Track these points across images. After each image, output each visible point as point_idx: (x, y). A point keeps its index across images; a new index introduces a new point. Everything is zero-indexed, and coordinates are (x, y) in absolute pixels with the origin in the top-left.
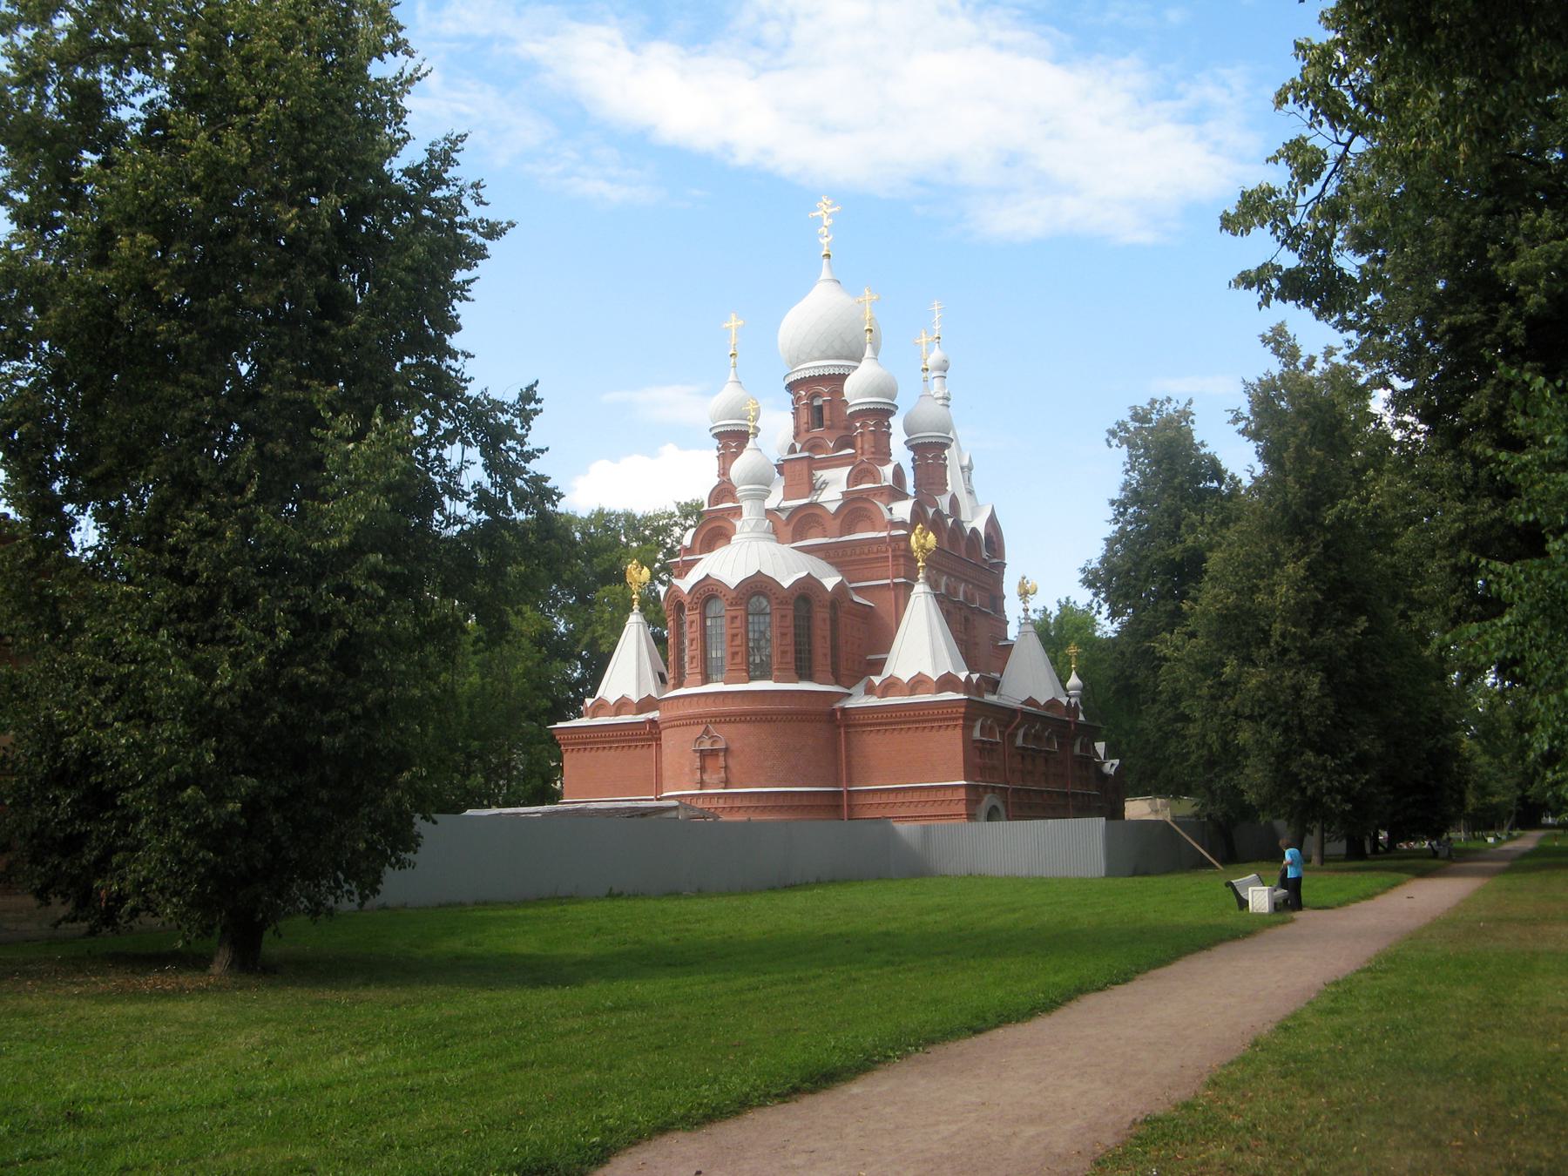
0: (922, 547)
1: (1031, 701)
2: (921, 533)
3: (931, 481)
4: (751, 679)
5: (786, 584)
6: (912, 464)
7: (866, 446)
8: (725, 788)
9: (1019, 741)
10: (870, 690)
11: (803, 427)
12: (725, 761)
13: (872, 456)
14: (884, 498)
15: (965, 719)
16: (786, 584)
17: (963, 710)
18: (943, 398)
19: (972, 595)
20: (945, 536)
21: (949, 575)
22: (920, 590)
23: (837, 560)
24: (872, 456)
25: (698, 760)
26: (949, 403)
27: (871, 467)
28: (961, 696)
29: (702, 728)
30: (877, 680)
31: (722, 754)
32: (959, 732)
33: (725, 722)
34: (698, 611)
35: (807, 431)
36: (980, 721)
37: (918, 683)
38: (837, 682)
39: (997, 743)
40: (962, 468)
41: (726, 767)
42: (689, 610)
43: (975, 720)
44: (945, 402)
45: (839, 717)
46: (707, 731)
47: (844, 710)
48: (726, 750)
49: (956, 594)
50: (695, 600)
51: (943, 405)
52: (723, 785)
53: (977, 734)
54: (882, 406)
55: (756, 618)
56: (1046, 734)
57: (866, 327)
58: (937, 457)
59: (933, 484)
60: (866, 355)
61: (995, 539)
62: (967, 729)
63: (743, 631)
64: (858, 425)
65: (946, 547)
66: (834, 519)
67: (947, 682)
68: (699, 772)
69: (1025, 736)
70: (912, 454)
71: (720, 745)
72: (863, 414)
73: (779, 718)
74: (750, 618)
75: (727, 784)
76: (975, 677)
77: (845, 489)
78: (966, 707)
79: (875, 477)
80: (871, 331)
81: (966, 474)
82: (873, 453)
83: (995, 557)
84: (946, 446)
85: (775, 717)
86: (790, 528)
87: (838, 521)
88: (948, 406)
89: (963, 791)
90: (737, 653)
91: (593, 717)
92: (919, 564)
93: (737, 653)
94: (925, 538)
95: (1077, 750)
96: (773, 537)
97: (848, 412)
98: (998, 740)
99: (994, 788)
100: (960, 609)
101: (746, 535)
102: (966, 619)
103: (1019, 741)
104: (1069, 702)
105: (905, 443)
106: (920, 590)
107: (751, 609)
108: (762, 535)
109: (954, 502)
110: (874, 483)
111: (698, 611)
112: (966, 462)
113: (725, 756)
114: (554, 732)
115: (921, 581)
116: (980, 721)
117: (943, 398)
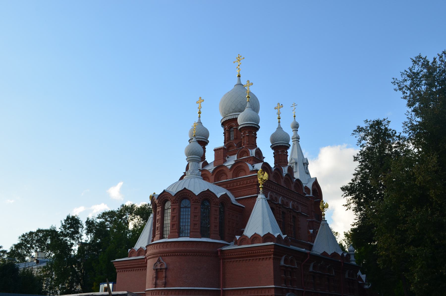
0: (262, 179)
1: (325, 253)
2: (261, 173)
3: (280, 161)
4: (179, 237)
5: (197, 194)
6: (273, 155)
7: (245, 142)
8: (165, 287)
9: (311, 269)
10: (236, 243)
11: (227, 139)
12: (165, 274)
13: (247, 146)
14: (251, 162)
15: (274, 254)
16: (197, 194)
17: (273, 250)
18: (296, 138)
19: (297, 206)
20: (272, 175)
21: (283, 196)
22: (261, 196)
23: (230, 188)
24: (247, 146)
25: (155, 273)
26: (299, 140)
27: (246, 149)
28: (272, 243)
29: (158, 258)
30: (238, 237)
31: (164, 271)
32: (271, 261)
33: (167, 256)
34: (161, 207)
35: (228, 141)
36: (284, 256)
37: (255, 237)
38: (222, 239)
39: (295, 268)
40: (304, 164)
41: (166, 277)
42: (158, 207)
43: (282, 256)
44: (297, 140)
45: (219, 254)
46: (159, 261)
47: (222, 251)
48: (166, 269)
49: (287, 204)
50: (160, 202)
51: (296, 141)
52: (164, 285)
53: (282, 263)
54: (252, 125)
55: (185, 210)
56: (328, 266)
57: (247, 96)
58: (283, 151)
59: (281, 162)
60: (247, 106)
61: (318, 191)
62: (276, 260)
63: (177, 214)
64: (242, 134)
65: (272, 179)
66: (230, 171)
67: (268, 237)
68: (155, 279)
69: (314, 267)
70: (273, 151)
71: (164, 267)
72: (245, 128)
73: (190, 254)
74: (182, 210)
75: (165, 285)
76: (284, 237)
77: (236, 159)
78: (274, 248)
79: (248, 153)
80: (249, 97)
81: (306, 166)
82: (248, 144)
83: (318, 199)
84: (288, 148)
85: (188, 254)
86: (213, 176)
87: (232, 172)
88: (299, 141)
89: (273, 290)
90: (174, 225)
91: (130, 257)
92: (260, 186)
93: (174, 225)
94: (263, 175)
95: (347, 276)
96: (201, 177)
97: (239, 128)
98: (296, 267)
99: (293, 291)
100: (290, 212)
101: (188, 176)
102: (294, 216)
103: (311, 269)
104: (342, 254)
105: (271, 147)
106: (261, 196)
107: (181, 206)
108: (195, 176)
109: (290, 170)
110: (248, 156)
111: (161, 207)
112: (305, 161)
113: (165, 272)
114: (114, 263)
115: (261, 193)
116: (284, 256)
117: (296, 138)
